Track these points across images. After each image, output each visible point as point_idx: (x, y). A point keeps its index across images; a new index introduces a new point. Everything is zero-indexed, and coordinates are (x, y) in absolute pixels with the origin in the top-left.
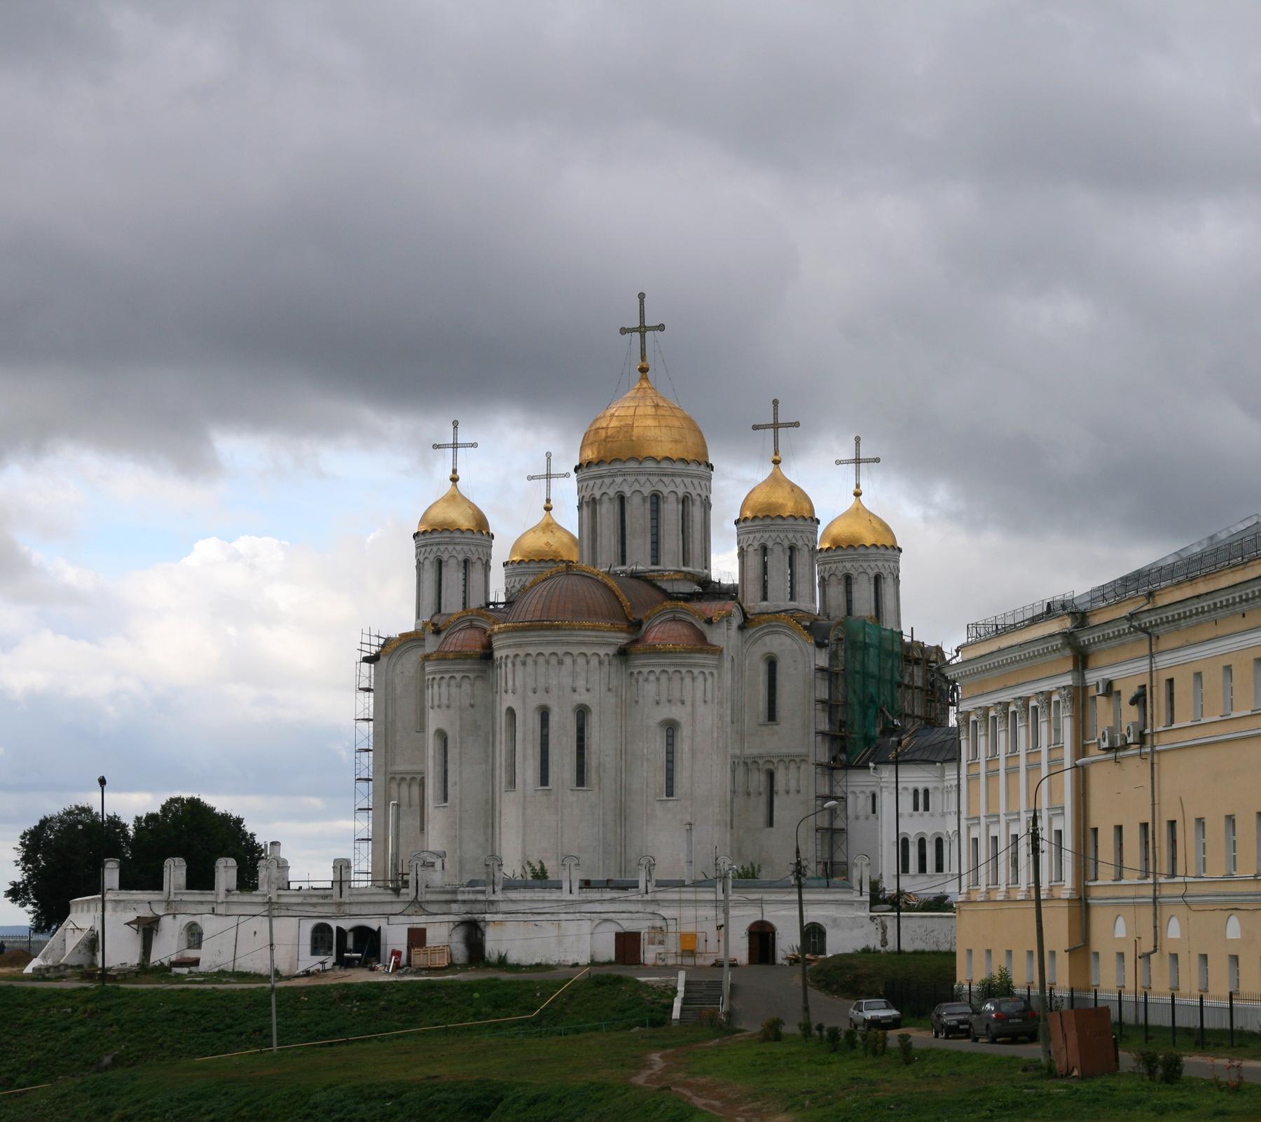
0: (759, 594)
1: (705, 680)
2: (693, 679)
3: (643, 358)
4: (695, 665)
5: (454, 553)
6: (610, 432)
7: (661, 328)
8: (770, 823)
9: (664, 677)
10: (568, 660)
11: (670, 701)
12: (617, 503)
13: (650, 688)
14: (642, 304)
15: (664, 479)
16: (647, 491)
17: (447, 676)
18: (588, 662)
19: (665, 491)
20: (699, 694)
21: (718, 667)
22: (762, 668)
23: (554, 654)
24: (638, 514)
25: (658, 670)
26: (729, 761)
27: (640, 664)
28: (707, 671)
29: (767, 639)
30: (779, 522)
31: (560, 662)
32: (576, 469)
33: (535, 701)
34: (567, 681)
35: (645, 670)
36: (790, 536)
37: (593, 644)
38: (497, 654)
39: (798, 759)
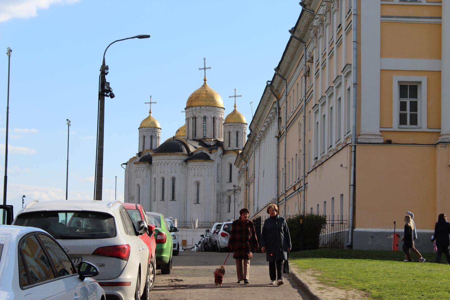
2: (205, 169)
3: (205, 77)
6: (193, 99)
7: (210, 68)
8: (229, 212)
9: (200, 168)
10: (170, 164)
14: (205, 61)
16: (202, 115)
18: (175, 164)
19: (207, 116)
21: (212, 166)
24: (200, 121)
25: (194, 167)
26: (216, 193)
27: (191, 164)
29: (229, 158)
31: (168, 164)
32: (185, 109)
35: (191, 167)
37: (177, 159)
38: (153, 162)
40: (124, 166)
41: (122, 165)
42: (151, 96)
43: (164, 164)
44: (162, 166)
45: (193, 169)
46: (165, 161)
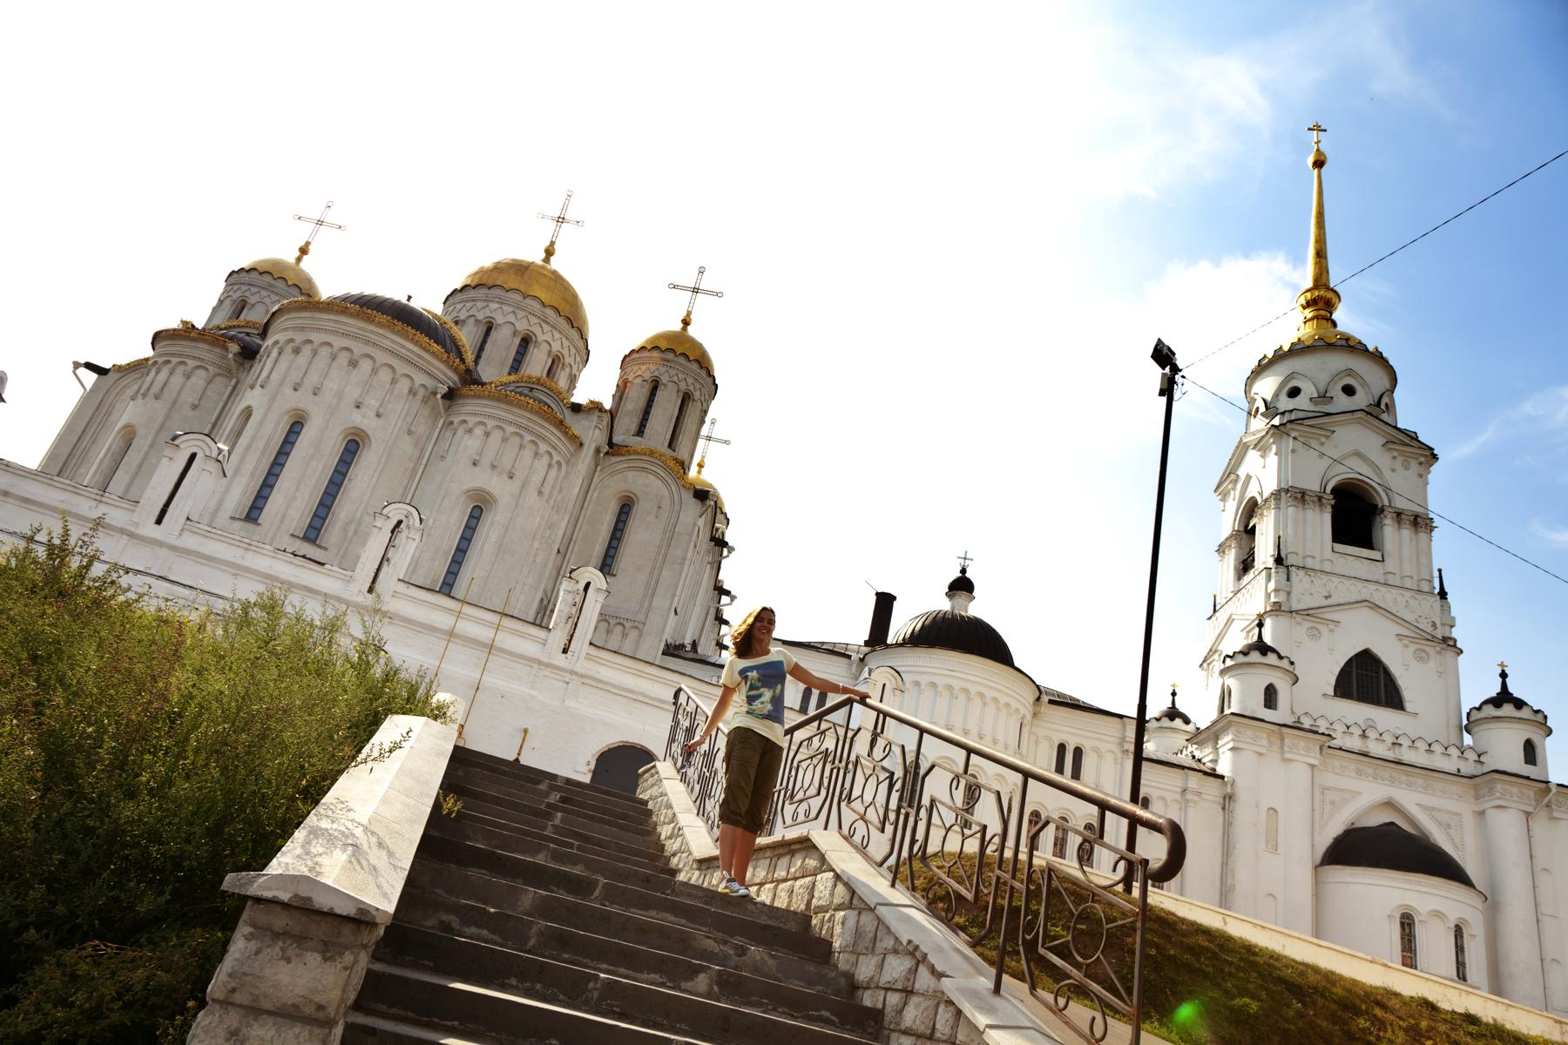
0: (634, 427)
1: (550, 466)
4: (544, 439)
5: (267, 300)
10: (366, 366)
11: (493, 467)
12: (482, 330)
13: (470, 444)
16: (522, 326)
17: (175, 360)
18: (394, 381)
19: (541, 337)
20: (536, 479)
21: (568, 463)
23: (347, 349)
25: (491, 423)
28: (556, 458)
29: (631, 475)
30: (682, 360)
31: (353, 364)
33: (292, 400)
34: (353, 393)
35: (472, 420)
36: (690, 381)
39: (628, 625)
40: (90, 378)
41: (77, 365)
43: (334, 357)
44: (322, 361)
45: (479, 431)
46: (347, 343)
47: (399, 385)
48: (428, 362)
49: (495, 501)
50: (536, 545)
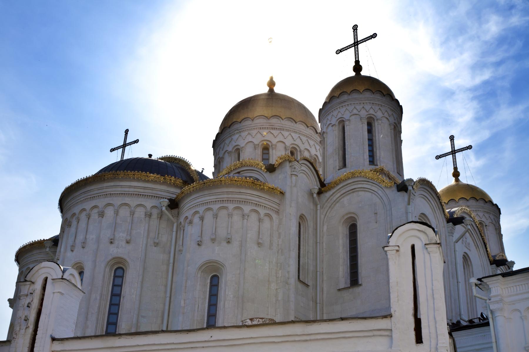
1: (260, 220)
4: (246, 202)
11: (213, 240)
15: (273, 132)
18: (132, 213)
19: (274, 141)
20: (252, 234)
21: (277, 212)
22: (343, 233)
23: (95, 207)
25: (201, 209)
28: (262, 211)
29: (346, 200)
31: (102, 214)
34: (107, 234)
37: (139, 195)
42: (127, 132)
45: (196, 220)
47: (136, 215)
48: (152, 189)
49: (223, 265)
50: (273, 286)
